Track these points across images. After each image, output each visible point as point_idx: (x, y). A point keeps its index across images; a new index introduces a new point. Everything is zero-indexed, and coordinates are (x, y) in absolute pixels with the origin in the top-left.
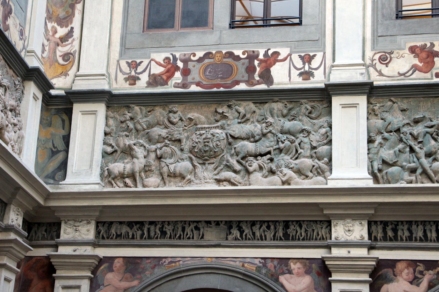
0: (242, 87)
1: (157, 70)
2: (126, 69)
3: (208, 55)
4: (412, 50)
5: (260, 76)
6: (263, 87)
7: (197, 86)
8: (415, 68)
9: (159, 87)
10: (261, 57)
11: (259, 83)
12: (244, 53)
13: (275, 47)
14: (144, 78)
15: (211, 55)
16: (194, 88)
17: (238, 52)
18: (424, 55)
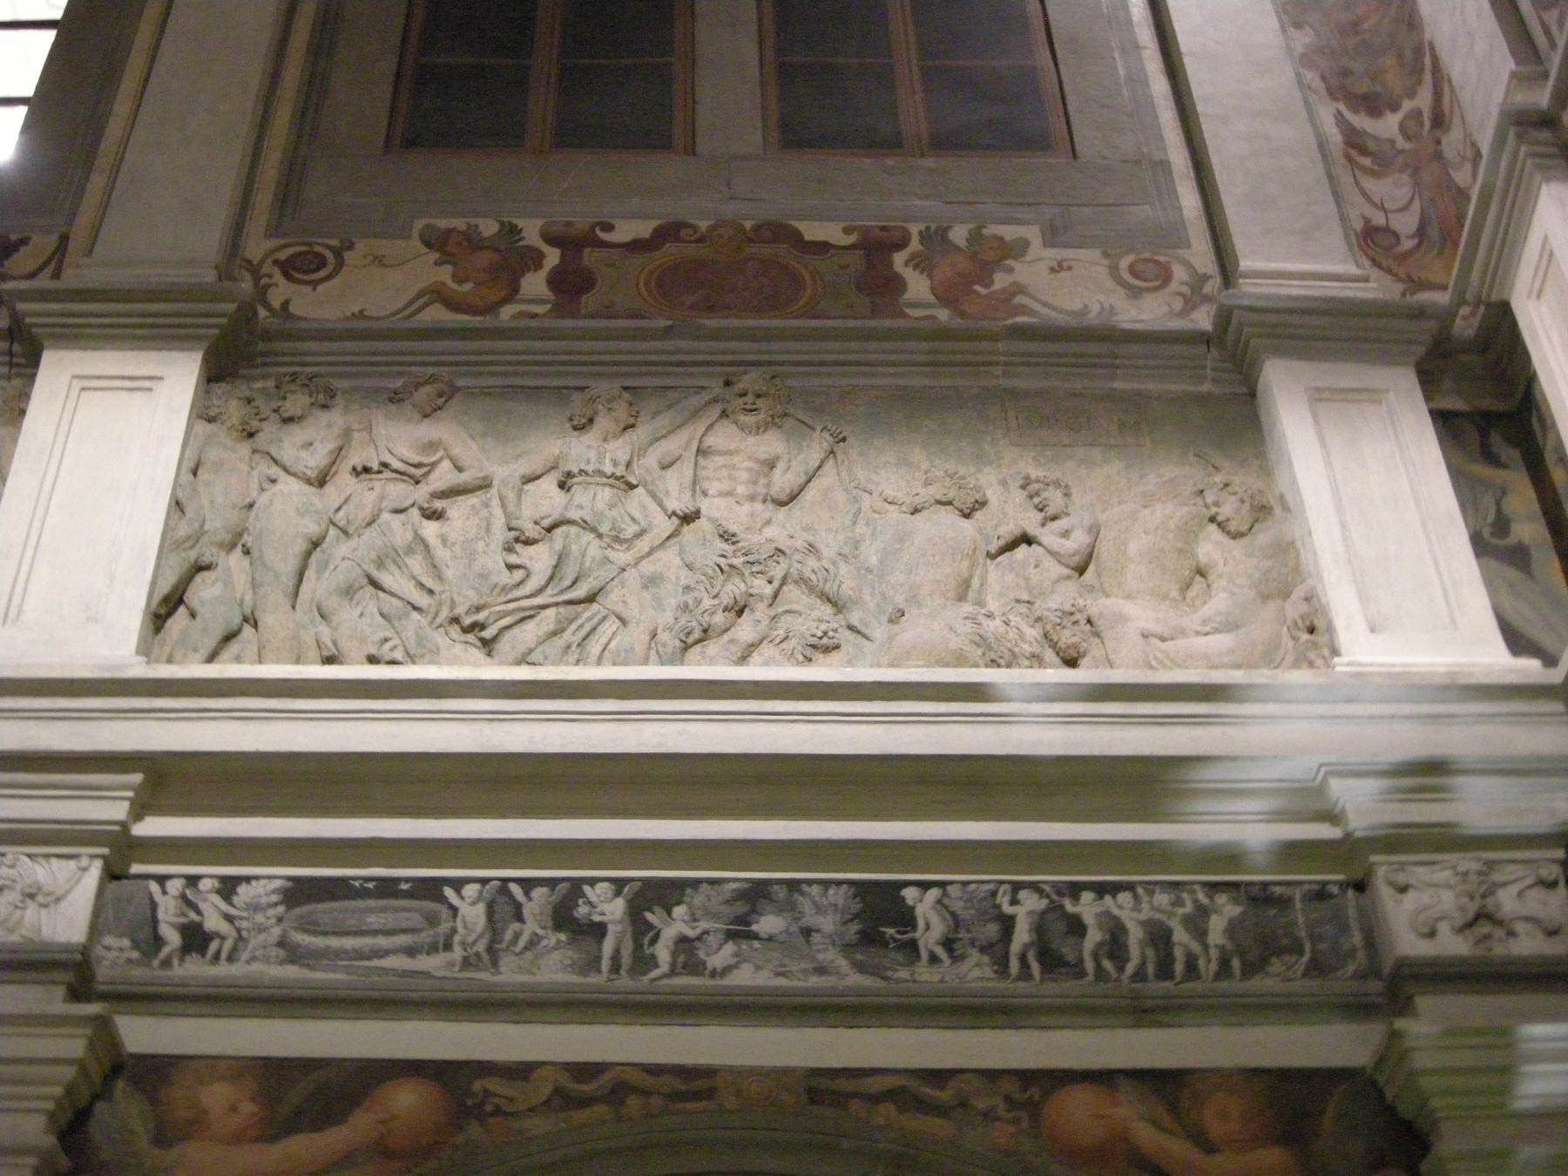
4: (437, 242)
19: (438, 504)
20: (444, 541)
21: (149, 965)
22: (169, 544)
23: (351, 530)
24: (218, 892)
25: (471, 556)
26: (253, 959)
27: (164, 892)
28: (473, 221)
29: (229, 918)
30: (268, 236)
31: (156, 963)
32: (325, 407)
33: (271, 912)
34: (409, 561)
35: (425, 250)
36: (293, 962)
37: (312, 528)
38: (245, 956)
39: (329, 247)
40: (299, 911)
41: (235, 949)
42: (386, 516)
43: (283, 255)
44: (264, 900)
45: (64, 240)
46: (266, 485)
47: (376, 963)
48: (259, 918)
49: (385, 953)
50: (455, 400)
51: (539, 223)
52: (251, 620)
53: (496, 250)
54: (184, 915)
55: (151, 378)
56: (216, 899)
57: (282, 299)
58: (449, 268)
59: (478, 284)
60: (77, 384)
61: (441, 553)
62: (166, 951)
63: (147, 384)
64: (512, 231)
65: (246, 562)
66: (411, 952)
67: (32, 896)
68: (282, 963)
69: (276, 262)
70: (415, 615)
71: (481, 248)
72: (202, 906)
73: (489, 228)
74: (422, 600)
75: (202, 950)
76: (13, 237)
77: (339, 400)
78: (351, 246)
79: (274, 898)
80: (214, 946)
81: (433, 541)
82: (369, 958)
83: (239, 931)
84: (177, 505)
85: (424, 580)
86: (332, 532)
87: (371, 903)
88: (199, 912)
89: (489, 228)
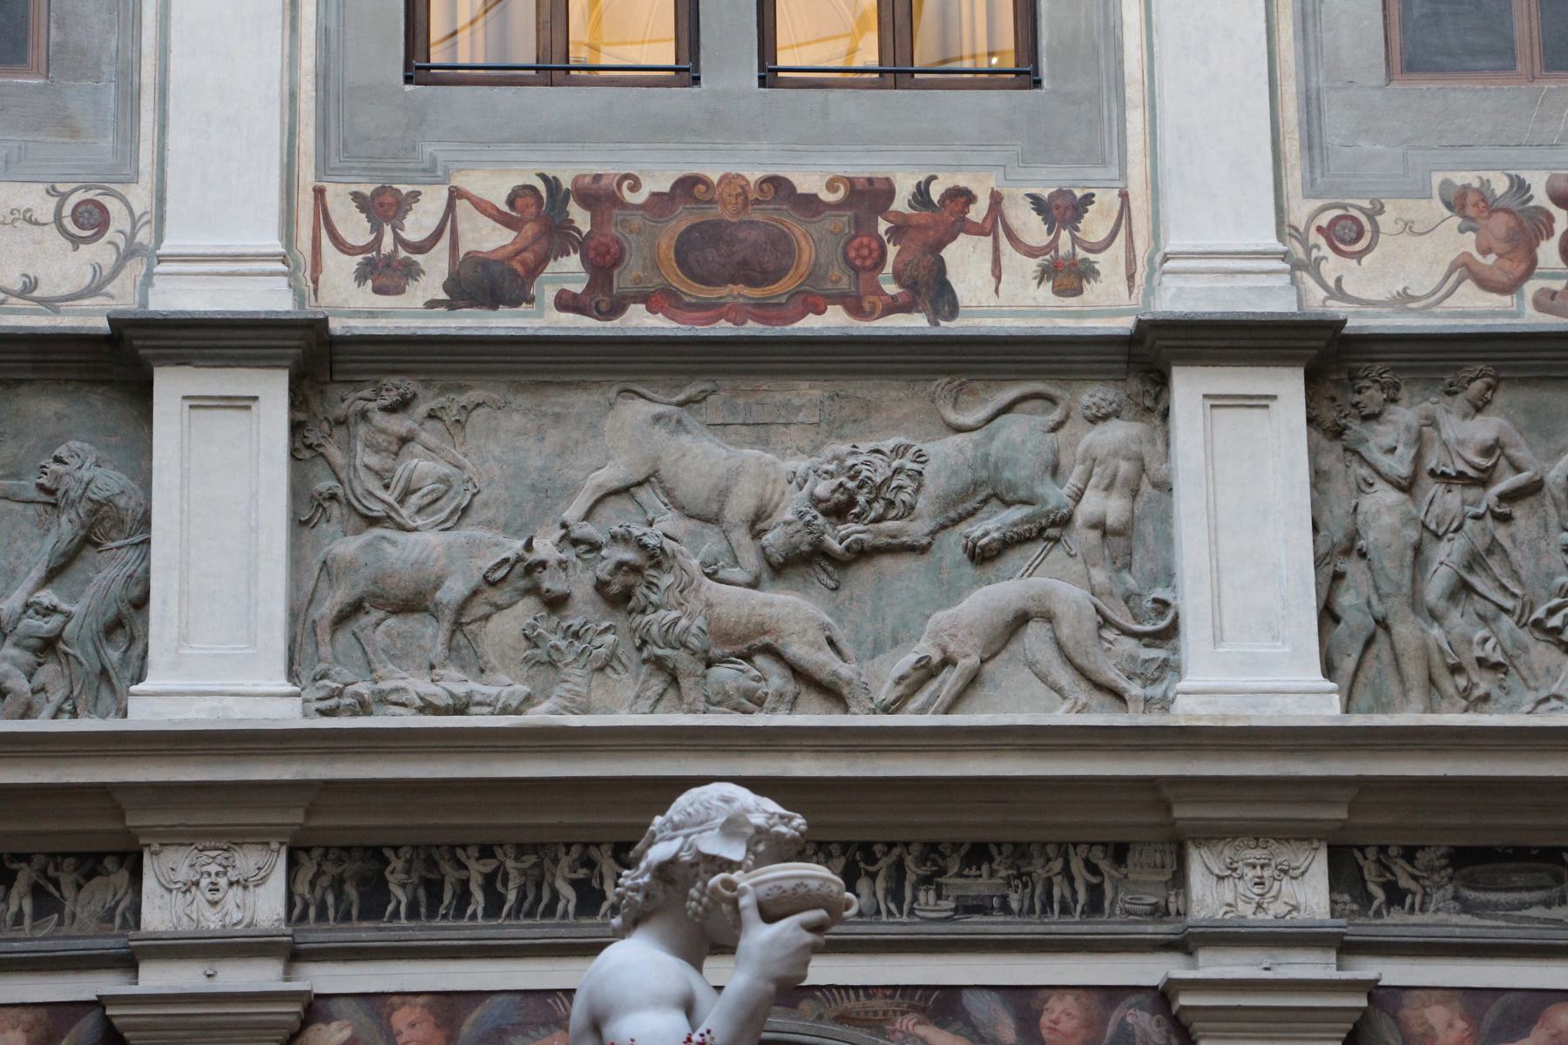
0: (833, 321)
1: (487, 238)
2: (356, 228)
3: (687, 186)
4: (1457, 201)
5: (897, 277)
6: (915, 323)
7: (652, 310)
8: (1465, 269)
9: (503, 309)
10: (901, 204)
11: (894, 307)
12: (831, 186)
13: (958, 167)
14: (435, 269)
15: (702, 187)
16: (640, 321)
17: (808, 181)
18: (1500, 223)
19: (1505, 509)
20: (1513, 538)
21: (1367, 916)
22: (1318, 563)
23: (1441, 531)
24: (1403, 857)
25: (1537, 555)
26: (1437, 910)
27: (1366, 858)
28: (1486, 175)
29: (1415, 878)
30: (1306, 197)
31: (1371, 913)
32: (1394, 401)
33: (1443, 873)
34: (1490, 562)
35: (1447, 213)
36: (1466, 912)
37: (1413, 534)
38: (1432, 908)
39: (1361, 209)
40: (1464, 871)
41: (1423, 903)
42: (1469, 523)
43: (1324, 220)
44: (1437, 863)
45: (1124, 196)
46: (1363, 487)
47: (1524, 913)
48: (1436, 877)
49: (1531, 905)
50: (1500, 393)
51: (1545, 176)
52: (1382, 623)
53: (1507, 211)
54: (1381, 875)
55: (1267, 397)
56: (1401, 862)
57: (1335, 276)
58: (1471, 236)
59: (1500, 256)
60: (1209, 402)
61: (1515, 555)
62: (1376, 903)
63: (1264, 402)
64: (1520, 187)
65: (1363, 564)
66: (1548, 904)
67: (1285, 872)
68: (1458, 913)
69: (1319, 229)
70: (1505, 617)
71: (1496, 210)
72: (1395, 868)
73: (1500, 185)
74: (1509, 603)
75: (1402, 904)
76: (1079, 193)
77: (1404, 394)
78: (1381, 211)
79: (1443, 862)
80: (1408, 900)
81: (1507, 544)
82: (1518, 909)
83: (1424, 888)
84: (1315, 529)
85: (1504, 581)
86: (1426, 534)
87: (1513, 865)
88: (1393, 874)
89: (1500, 185)
